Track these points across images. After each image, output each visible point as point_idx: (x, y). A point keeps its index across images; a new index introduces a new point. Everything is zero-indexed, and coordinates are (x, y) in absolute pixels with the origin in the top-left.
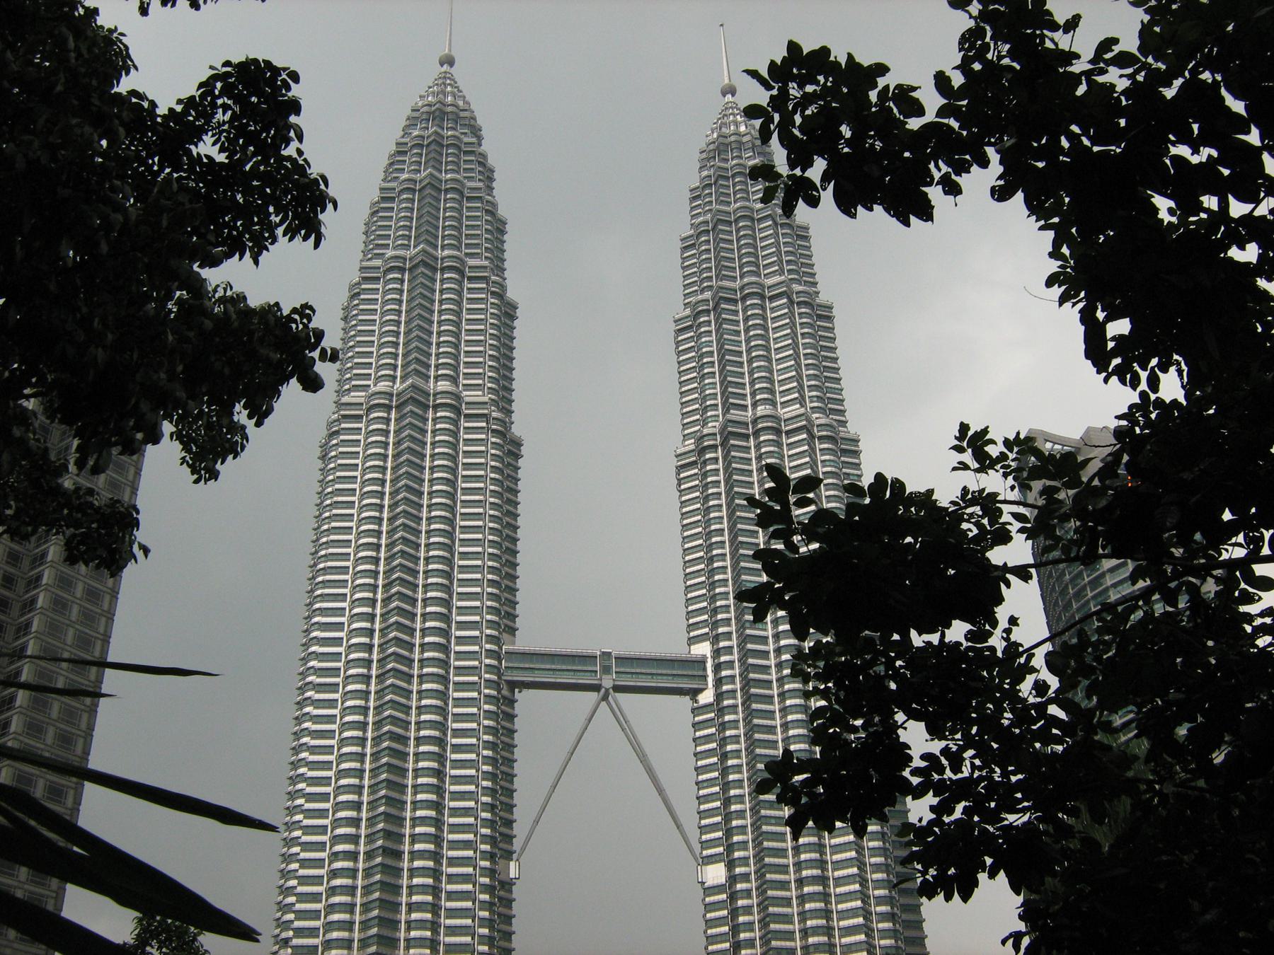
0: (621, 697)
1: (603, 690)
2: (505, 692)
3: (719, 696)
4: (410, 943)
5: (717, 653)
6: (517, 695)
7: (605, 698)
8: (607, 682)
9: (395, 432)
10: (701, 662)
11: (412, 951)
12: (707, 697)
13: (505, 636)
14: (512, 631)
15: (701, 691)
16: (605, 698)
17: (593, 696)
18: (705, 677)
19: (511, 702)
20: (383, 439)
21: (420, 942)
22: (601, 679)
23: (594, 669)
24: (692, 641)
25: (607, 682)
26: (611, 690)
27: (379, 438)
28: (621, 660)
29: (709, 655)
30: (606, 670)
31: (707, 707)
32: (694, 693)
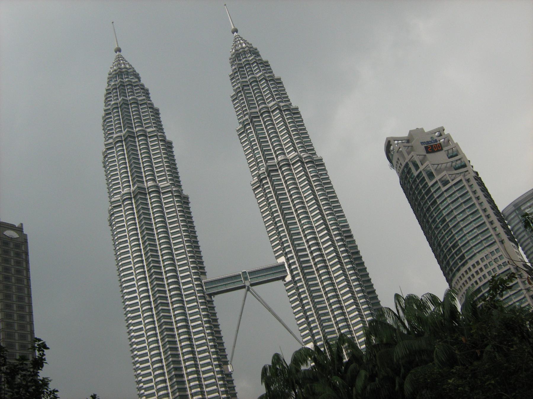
0: (254, 288)
1: (247, 287)
2: (208, 299)
3: (293, 277)
4: (193, 395)
5: (288, 260)
6: (213, 298)
7: (248, 290)
8: (247, 284)
9: (138, 218)
10: (283, 265)
11: (194, 398)
12: (288, 278)
13: (202, 277)
14: (204, 273)
15: (286, 276)
16: (248, 290)
17: (244, 290)
18: (286, 271)
19: (211, 302)
20: (134, 222)
21: (196, 394)
22: (244, 283)
23: (241, 279)
25: (247, 284)
26: (250, 287)
27: (132, 222)
28: (251, 273)
29: (285, 262)
30: (246, 279)
32: (283, 278)
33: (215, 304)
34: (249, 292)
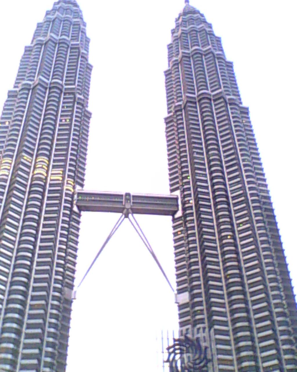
0: (135, 215)
2: (75, 209)
3: (185, 216)
8: (128, 206)
10: (176, 199)
12: (179, 214)
14: (82, 185)
15: (174, 212)
19: (79, 216)
22: (125, 205)
23: (121, 200)
24: (172, 191)
25: (128, 206)
26: (130, 211)
31: (179, 219)
32: (173, 213)
33: (82, 219)
34: (126, 219)
